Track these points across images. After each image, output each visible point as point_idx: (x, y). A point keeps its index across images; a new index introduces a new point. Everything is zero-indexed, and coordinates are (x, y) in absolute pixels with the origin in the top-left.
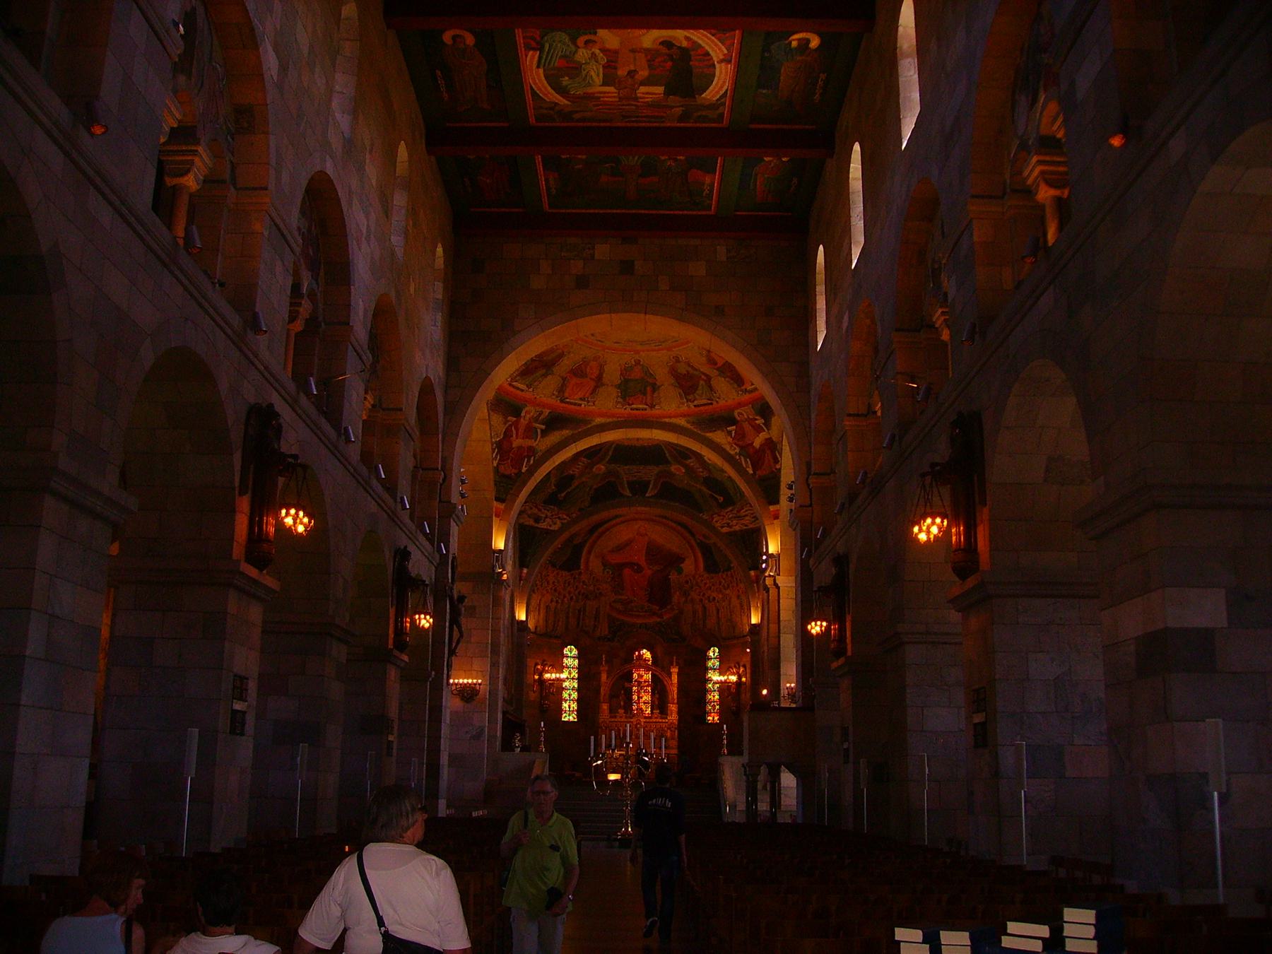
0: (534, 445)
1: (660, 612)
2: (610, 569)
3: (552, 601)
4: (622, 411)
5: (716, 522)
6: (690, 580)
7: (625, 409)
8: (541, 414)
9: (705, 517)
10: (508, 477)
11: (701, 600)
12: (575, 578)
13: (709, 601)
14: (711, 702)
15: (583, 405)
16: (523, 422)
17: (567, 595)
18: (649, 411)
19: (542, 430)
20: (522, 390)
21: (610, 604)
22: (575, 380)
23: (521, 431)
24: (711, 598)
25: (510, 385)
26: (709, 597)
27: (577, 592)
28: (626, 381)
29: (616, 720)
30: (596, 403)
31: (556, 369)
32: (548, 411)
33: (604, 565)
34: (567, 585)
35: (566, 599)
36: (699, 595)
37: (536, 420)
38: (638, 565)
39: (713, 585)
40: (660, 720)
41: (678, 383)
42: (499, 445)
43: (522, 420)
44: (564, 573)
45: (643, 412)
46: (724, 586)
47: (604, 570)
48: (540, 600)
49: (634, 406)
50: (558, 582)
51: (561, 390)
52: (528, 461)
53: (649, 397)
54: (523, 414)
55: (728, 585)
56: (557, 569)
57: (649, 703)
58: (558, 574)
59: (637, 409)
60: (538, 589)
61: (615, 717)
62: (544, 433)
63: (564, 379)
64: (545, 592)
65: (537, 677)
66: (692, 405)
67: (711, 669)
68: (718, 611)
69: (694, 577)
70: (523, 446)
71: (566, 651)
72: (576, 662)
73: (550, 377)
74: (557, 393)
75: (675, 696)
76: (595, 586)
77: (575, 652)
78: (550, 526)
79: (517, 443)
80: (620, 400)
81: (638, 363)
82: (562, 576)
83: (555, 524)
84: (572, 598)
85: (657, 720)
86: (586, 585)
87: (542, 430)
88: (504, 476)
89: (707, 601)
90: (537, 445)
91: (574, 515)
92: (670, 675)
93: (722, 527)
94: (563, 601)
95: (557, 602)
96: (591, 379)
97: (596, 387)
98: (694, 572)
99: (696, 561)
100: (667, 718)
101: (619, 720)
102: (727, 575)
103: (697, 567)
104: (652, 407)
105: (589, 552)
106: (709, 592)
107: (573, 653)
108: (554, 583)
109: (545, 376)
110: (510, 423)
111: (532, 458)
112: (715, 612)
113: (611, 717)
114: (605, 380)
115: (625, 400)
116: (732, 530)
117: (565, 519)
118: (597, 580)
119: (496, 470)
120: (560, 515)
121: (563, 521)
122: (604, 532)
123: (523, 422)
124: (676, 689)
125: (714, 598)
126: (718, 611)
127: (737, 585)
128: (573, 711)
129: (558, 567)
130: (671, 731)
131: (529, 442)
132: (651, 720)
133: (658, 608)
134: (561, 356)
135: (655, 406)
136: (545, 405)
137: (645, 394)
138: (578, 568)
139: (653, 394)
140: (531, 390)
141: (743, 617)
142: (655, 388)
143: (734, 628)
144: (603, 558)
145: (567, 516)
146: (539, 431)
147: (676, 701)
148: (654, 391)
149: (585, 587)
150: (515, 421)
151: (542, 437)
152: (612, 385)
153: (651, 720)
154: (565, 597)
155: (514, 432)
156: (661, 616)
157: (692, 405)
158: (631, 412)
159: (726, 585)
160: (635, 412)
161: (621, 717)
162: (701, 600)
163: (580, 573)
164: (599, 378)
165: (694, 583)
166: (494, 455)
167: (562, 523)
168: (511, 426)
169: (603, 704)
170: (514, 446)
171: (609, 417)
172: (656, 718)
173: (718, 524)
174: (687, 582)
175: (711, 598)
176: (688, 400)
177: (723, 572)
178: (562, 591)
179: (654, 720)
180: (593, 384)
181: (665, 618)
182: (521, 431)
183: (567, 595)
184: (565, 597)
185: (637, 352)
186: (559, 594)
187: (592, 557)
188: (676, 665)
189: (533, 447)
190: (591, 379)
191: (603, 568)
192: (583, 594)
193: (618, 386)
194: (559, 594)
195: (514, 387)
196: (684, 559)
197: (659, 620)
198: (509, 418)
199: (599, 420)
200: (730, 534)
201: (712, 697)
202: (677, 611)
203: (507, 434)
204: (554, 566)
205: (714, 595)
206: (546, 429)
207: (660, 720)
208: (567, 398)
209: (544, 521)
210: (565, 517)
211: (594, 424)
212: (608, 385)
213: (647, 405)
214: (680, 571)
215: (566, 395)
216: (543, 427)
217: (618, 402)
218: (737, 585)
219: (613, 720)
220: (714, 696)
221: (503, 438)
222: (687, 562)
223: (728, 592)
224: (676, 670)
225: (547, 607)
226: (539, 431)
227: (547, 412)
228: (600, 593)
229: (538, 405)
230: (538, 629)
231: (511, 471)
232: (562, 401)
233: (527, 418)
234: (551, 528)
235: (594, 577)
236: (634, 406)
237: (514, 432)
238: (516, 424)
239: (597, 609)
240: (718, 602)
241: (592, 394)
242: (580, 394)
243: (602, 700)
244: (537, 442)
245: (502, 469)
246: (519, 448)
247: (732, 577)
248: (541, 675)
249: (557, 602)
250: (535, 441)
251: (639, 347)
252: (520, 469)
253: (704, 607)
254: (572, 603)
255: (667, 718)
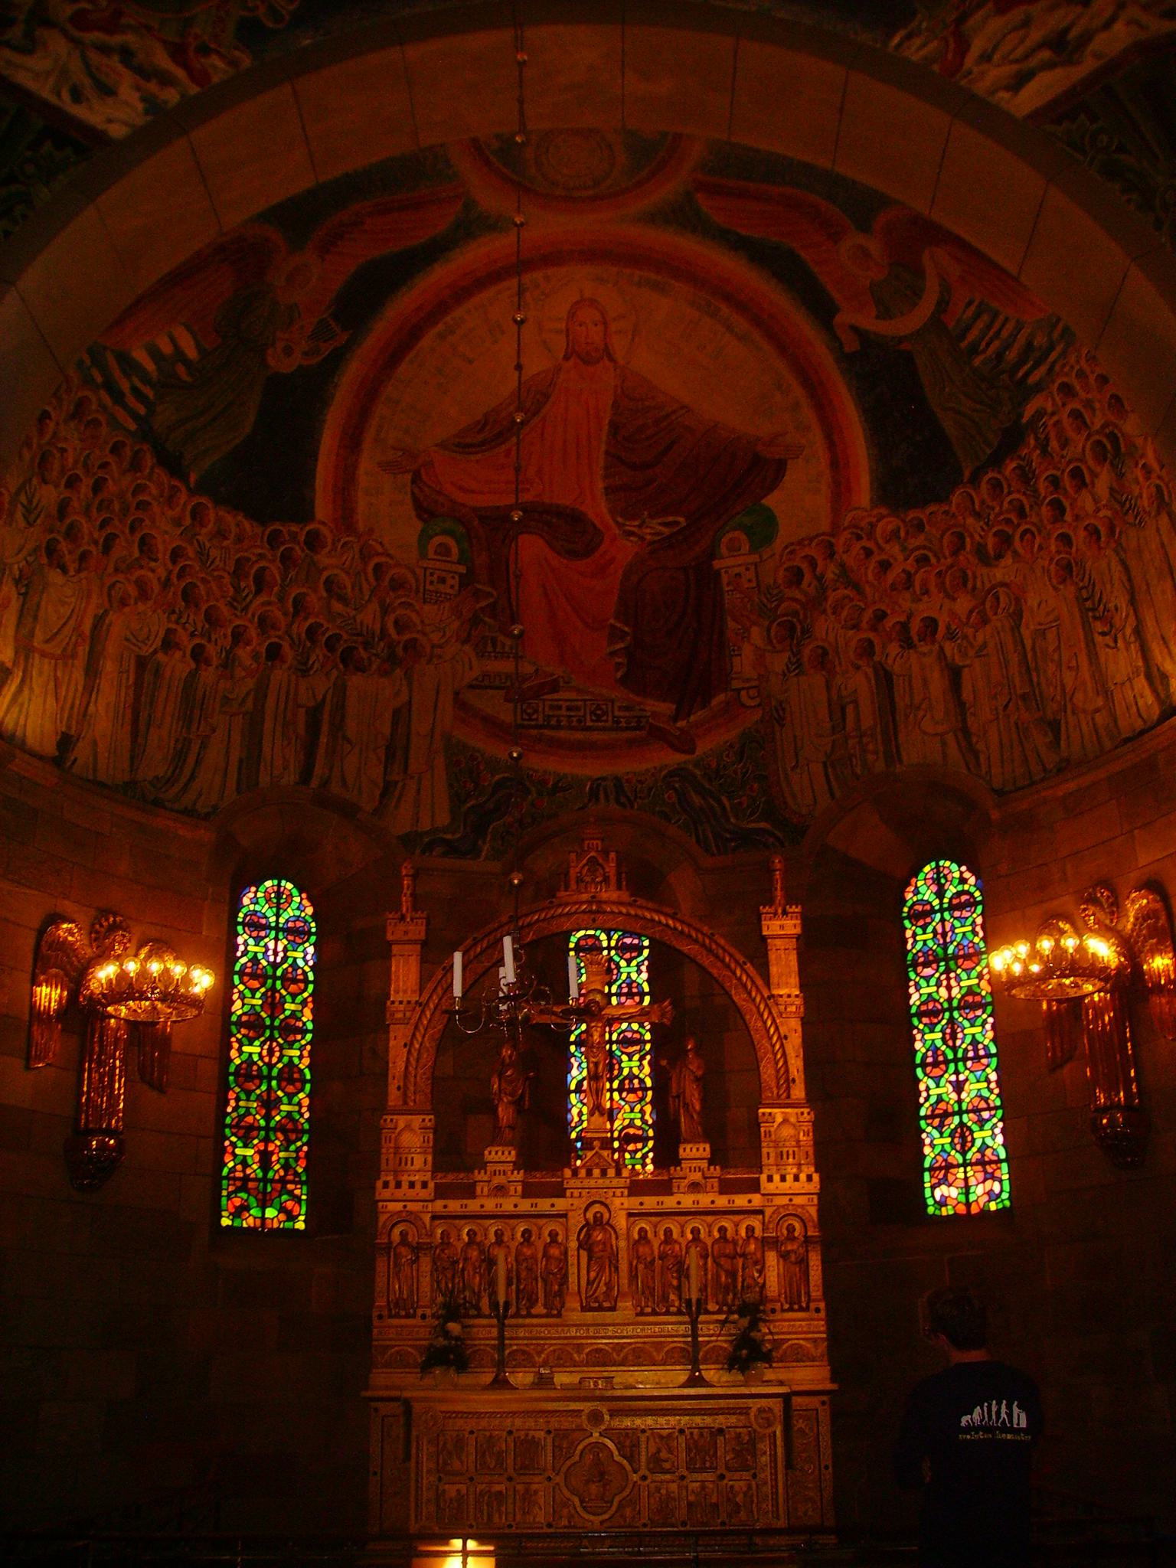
1: (681, 724)
2: (446, 532)
3: (169, 644)
5: (986, 58)
6: (812, 563)
9: (917, 51)
11: (867, 650)
12: (287, 559)
13: (907, 643)
14: (946, 1115)
17: (253, 632)
21: (457, 694)
24: (916, 626)
26: (904, 627)
27: (301, 628)
29: (473, 1206)
33: (425, 511)
34: (248, 584)
35: (244, 653)
36: (854, 627)
38: (575, 518)
39: (923, 560)
40: (722, 1202)
44: (233, 521)
46: (980, 552)
47: (424, 538)
48: (99, 621)
50: (202, 555)
55: (1005, 540)
56: (192, 492)
57: (644, 1140)
58: (197, 514)
60: (84, 557)
61: (469, 1192)
64: (132, 591)
65: (48, 995)
67: (930, 959)
68: (954, 675)
69: (831, 555)
71: (255, 901)
72: (304, 955)
75: (796, 1066)
76: (385, 610)
77: (298, 908)
78: (77, 96)
82: (221, 534)
83: (107, 91)
84: (274, 653)
85: (705, 1200)
86: (342, 599)
89: (894, 649)
91: (217, 67)
92: (758, 952)
93: (1019, 81)
94: (228, 664)
95: (198, 653)
98: (824, 526)
99: (838, 463)
100: (754, 1187)
101: (490, 1205)
102: (996, 486)
103: (841, 492)
105: (352, 442)
106: (905, 601)
107: (290, 912)
108: (176, 554)
112: (937, 682)
113: (441, 1192)
116: (1088, 65)
117: (166, 80)
118: (397, 585)
120: (130, 39)
121: (152, 87)
122: (410, 335)
124: (795, 1024)
125: (931, 624)
126: (954, 675)
127: (1058, 508)
128: (283, 1181)
129: (193, 478)
130: (784, 1256)
132: (669, 1202)
133: (666, 708)
138: (303, 512)
141: (1103, 653)
143: (1055, 727)
144: (416, 478)
145: (178, 53)
147: (798, 1092)
149: (338, 607)
153: (669, 1202)
154: (238, 636)
156: (684, 744)
159: (991, 542)
161: (500, 1190)
162: (867, 650)
163: (314, 542)
165: (831, 572)
167: (152, 104)
169: (402, 1121)
172: (695, 1187)
173: (996, 73)
174: (796, 577)
175: (916, 626)
177: (975, 480)
178: (224, 610)
179: (687, 1201)
181: (699, 752)
183: (253, 632)
184: (238, 636)
186: (212, 619)
187: (366, 465)
188: (790, 900)
191: (420, 525)
192: (330, 645)
194: (212, 619)
196: (781, 467)
197: (676, 759)
200: (1061, 109)
201: (946, 1090)
202: (756, 716)
204: (172, 464)
205: (932, 606)
207: (722, 1202)
209: (29, 46)
210: (163, 60)
214: (763, 530)
218: (1058, 508)
219: (454, 1206)
220: (959, 1087)
222: (794, 476)
223: (999, 574)
224: (791, 926)
225: (141, 663)
228: (411, 645)
230: (81, 752)
234: (78, 111)
235: (377, 566)
239: (396, 713)
240: (951, 636)
243: (394, 1097)
247: (1026, 476)
248: (76, 978)
249: (198, 653)
253: (885, 679)
254: (279, 675)
255: (754, 1187)
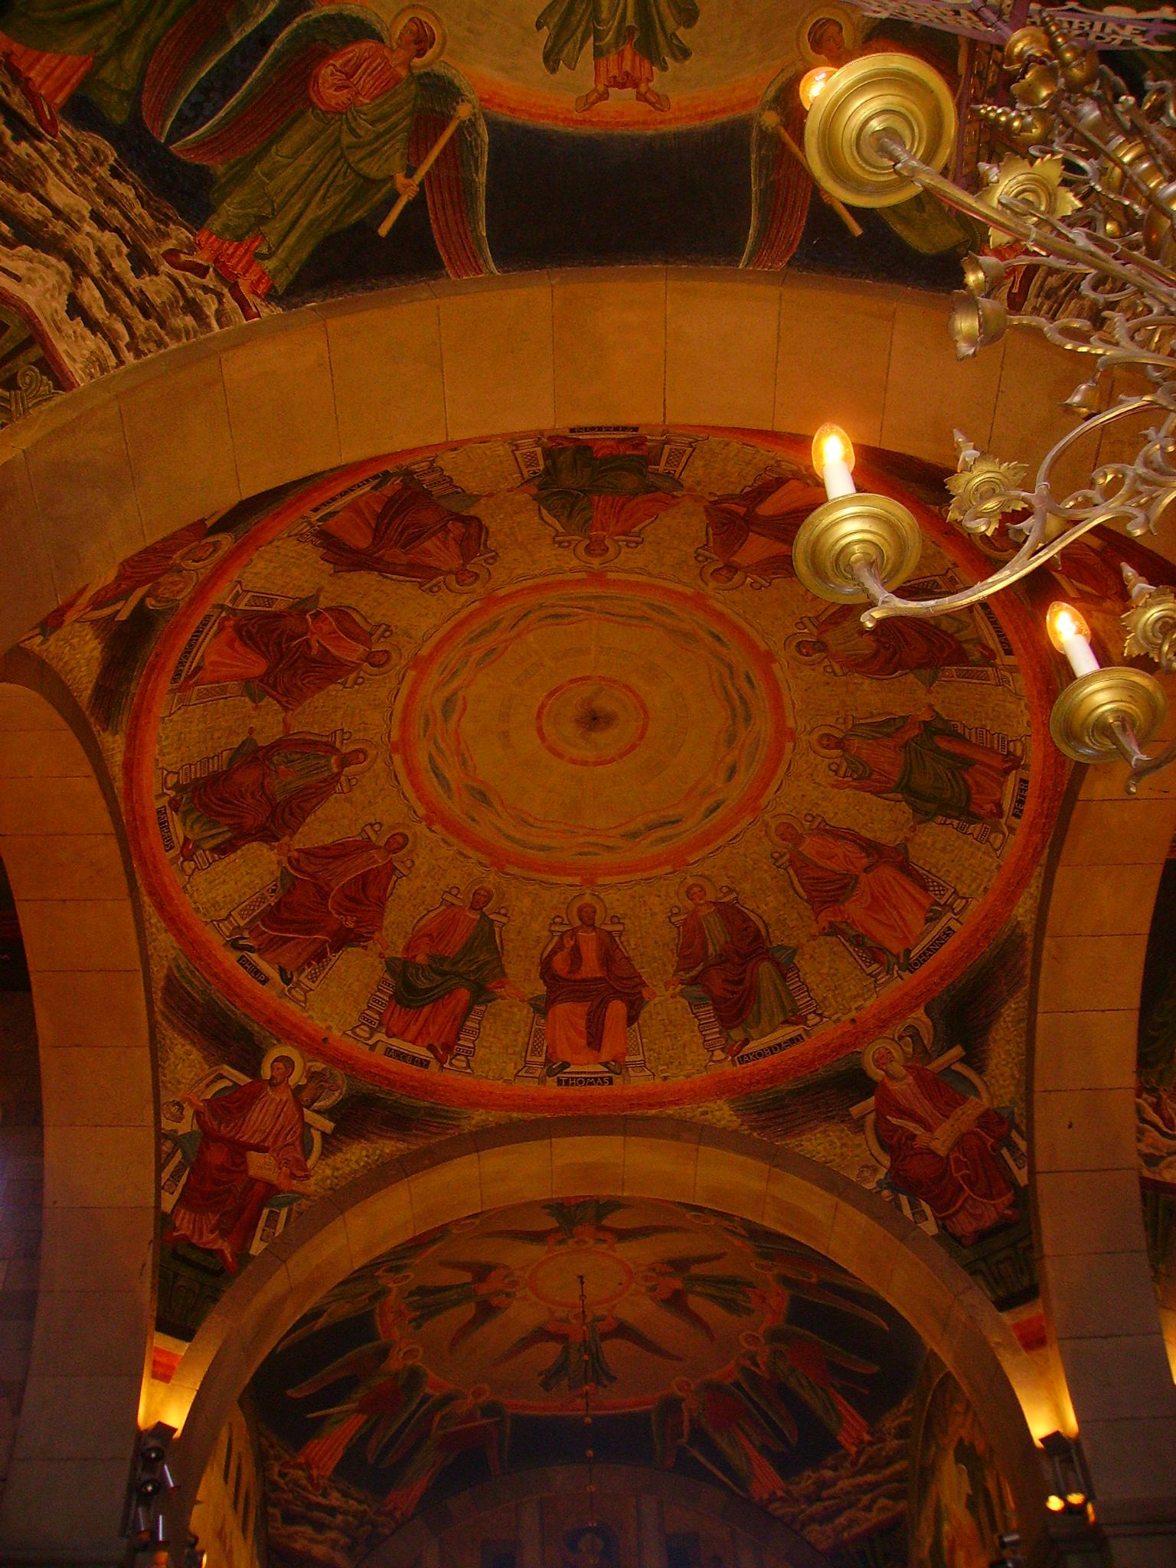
0: (985, 1102)
4: (1016, 840)
7: (1012, 830)
8: (915, 1034)
10: (1003, 1226)
15: (953, 925)
16: (903, 1087)
18: (1033, 775)
19: (963, 1060)
20: (792, 1041)
22: (854, 909)
23: (923, 1108)
25: (742, 1060)
28: (908, 790)
30: (963, 890)
31: (778, 937)
32: (920, 1012)
37: (928, 1056)
41: (920, 666)
42: (900, 1181)
43: (894, 1087)
45: (1033, 790)
49: (1007, 804)
51: (875, 953)
52: (1013, 1148)
53: (979, 757)
54: (876, 1074)
59: (1021, 802)
62: (975, 1059)
63: (834, 930)
66: (1010, 660)
70: (964, 1129)
73: (802, 963)
74: (875, 966)
79: (941, 1140)
80: (975, 828)
81: (830, 742)
87: (963, 1060)
88: (982, 1236)
90: (992, 1097)
96: (866, 870)
97: (905, 867)
104: (1013, 762)
109: (785, 970)
110: (872, 1116)
111: (1014, 1134)
114: (888, 837)
115: (973, 818)
119: (948, 1237)
123: (903, 1087)
131: (968, 1113)
134: (731, 913)
135: (1009, 752)
136: (897, 1010)
137: (967, 763)
139: (968, 742)
140: (813, 1020)
142: (936, 729)
146: (958, 1067)
148: (954, 735)
150: (877, 1100)
151: (980, 1070)
152: (913, 829)
155: (911, 1126)
157: (1003, 660)
158: (1025, 816)
160: (1030, 806)
164: (872, 848)
166: (907, 1211)
168: (880, 1119)
170: (942, 1152)
171: (1022, 882)
176: (989, 657)
180: (887, 873)
182: (923, 1108)
185: (784, 734)
189: (986, 1114)
190: (866, 870)
193: (923, 816)
195: (760, 1054)
198: (855, 1111)
199: (1023, 910)
203: (893, 1142)
206: (965, 1048)
208: (908, 951)
211: (1028, 929)
212: (907, 839)
213: (1006, 772)
215: (896, 947)
216: (957, 1051)
217: (983, 838)
221: (893, 1161)
226: (958, 1067)
227: (919, 1017)
229: (883, 1024)
231: (991, 1212)
232: (911, 968)
233: (897, 1068)
236: (1007, 804)
237: (911, 1126)
238: (889, 1104)
241: (925, 888)
242: (915, 920)
244: (985, 1095)
245: (965, 1225)
246: (960, 1142)
250: (978, 1094)
251: (763, 726)
252: (1013, 1184)
